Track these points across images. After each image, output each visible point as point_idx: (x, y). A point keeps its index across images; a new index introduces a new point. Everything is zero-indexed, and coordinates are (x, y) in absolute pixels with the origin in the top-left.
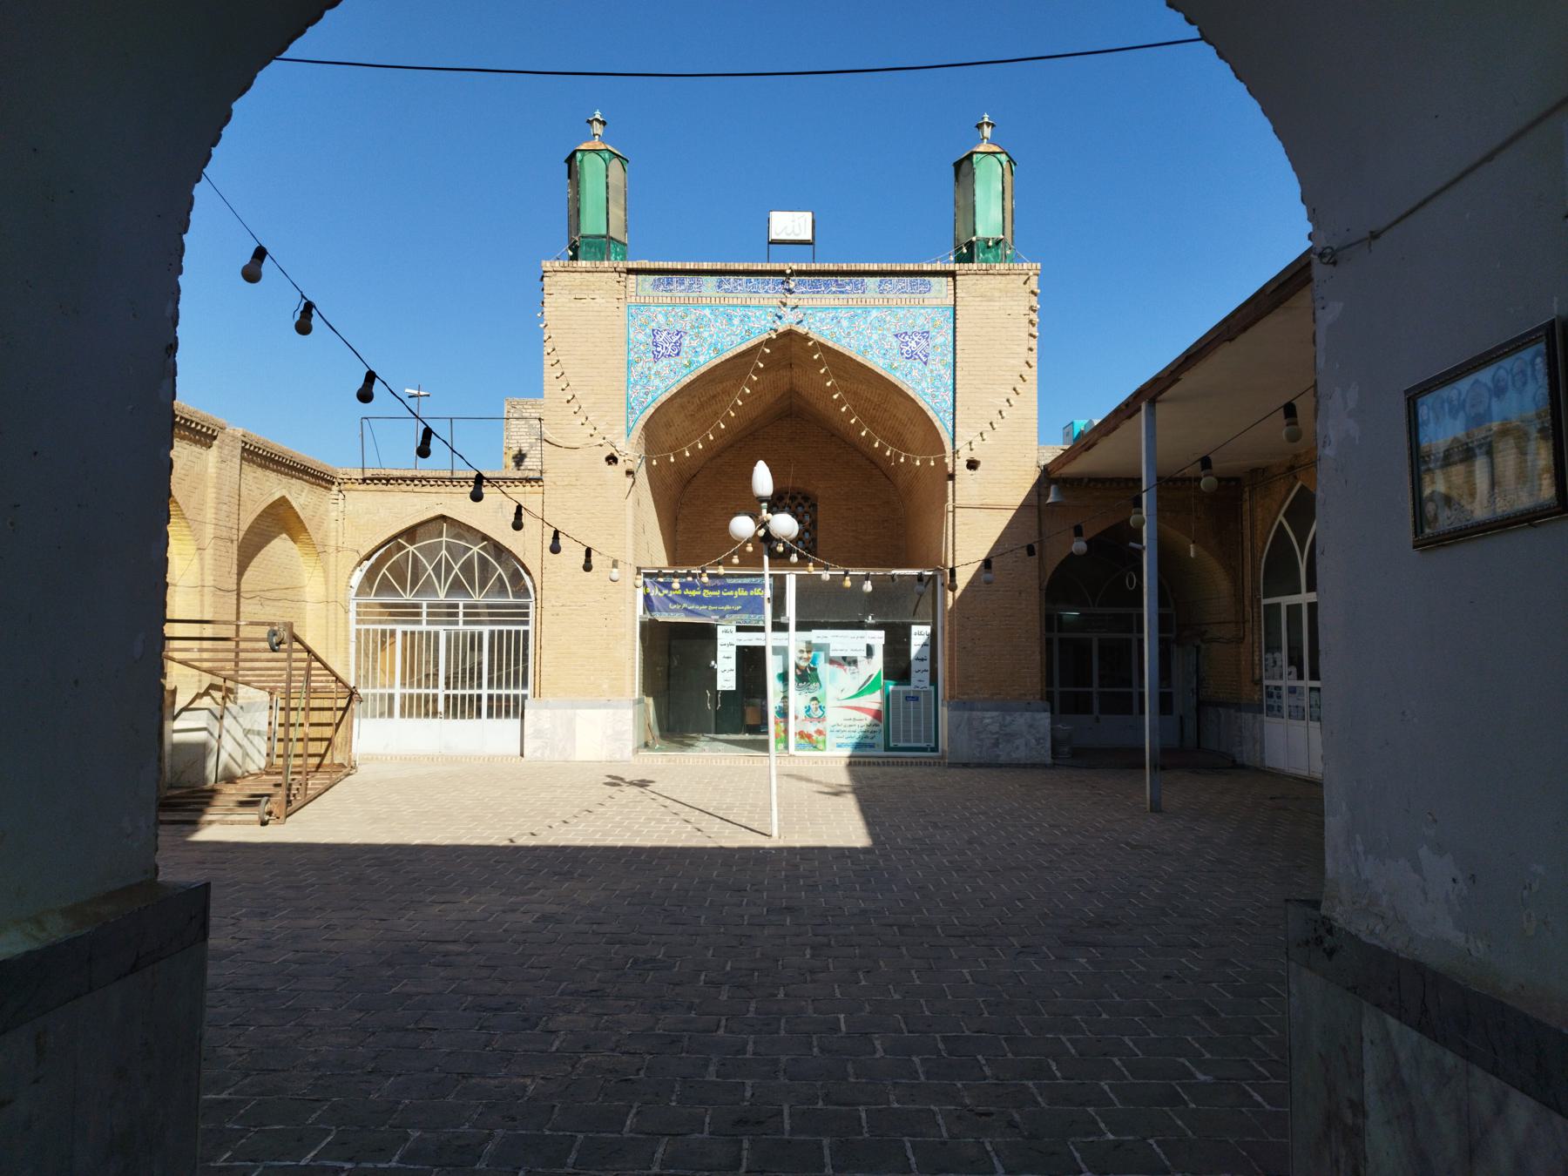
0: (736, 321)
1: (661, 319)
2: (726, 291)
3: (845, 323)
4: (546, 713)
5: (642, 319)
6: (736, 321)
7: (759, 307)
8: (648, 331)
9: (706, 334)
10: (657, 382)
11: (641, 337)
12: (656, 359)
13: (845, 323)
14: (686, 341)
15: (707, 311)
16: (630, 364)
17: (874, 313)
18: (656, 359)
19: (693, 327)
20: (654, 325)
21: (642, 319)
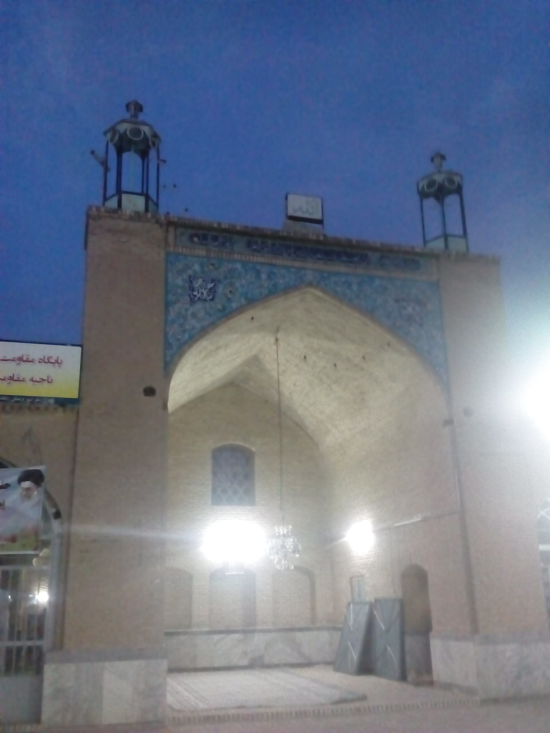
0: (264, 276)
1: (197, 267)
2: (255, 250)
3: (355, 287)
4: (70, 669)
5: (180, 266)
6: (264, 276)
7: (287, 268)
8: (185, 276)
9: (237, 284)
10: (193, 322)
11: (179, 281)
12: (193, 301)
13: (355, 287)
14: (220, 289)
15: (238, 266)
16: (167, 305)
17: (377, 282)
18: (193, 301)
19: (226, 278)
20: (190, 272)
21: (180, 266)
